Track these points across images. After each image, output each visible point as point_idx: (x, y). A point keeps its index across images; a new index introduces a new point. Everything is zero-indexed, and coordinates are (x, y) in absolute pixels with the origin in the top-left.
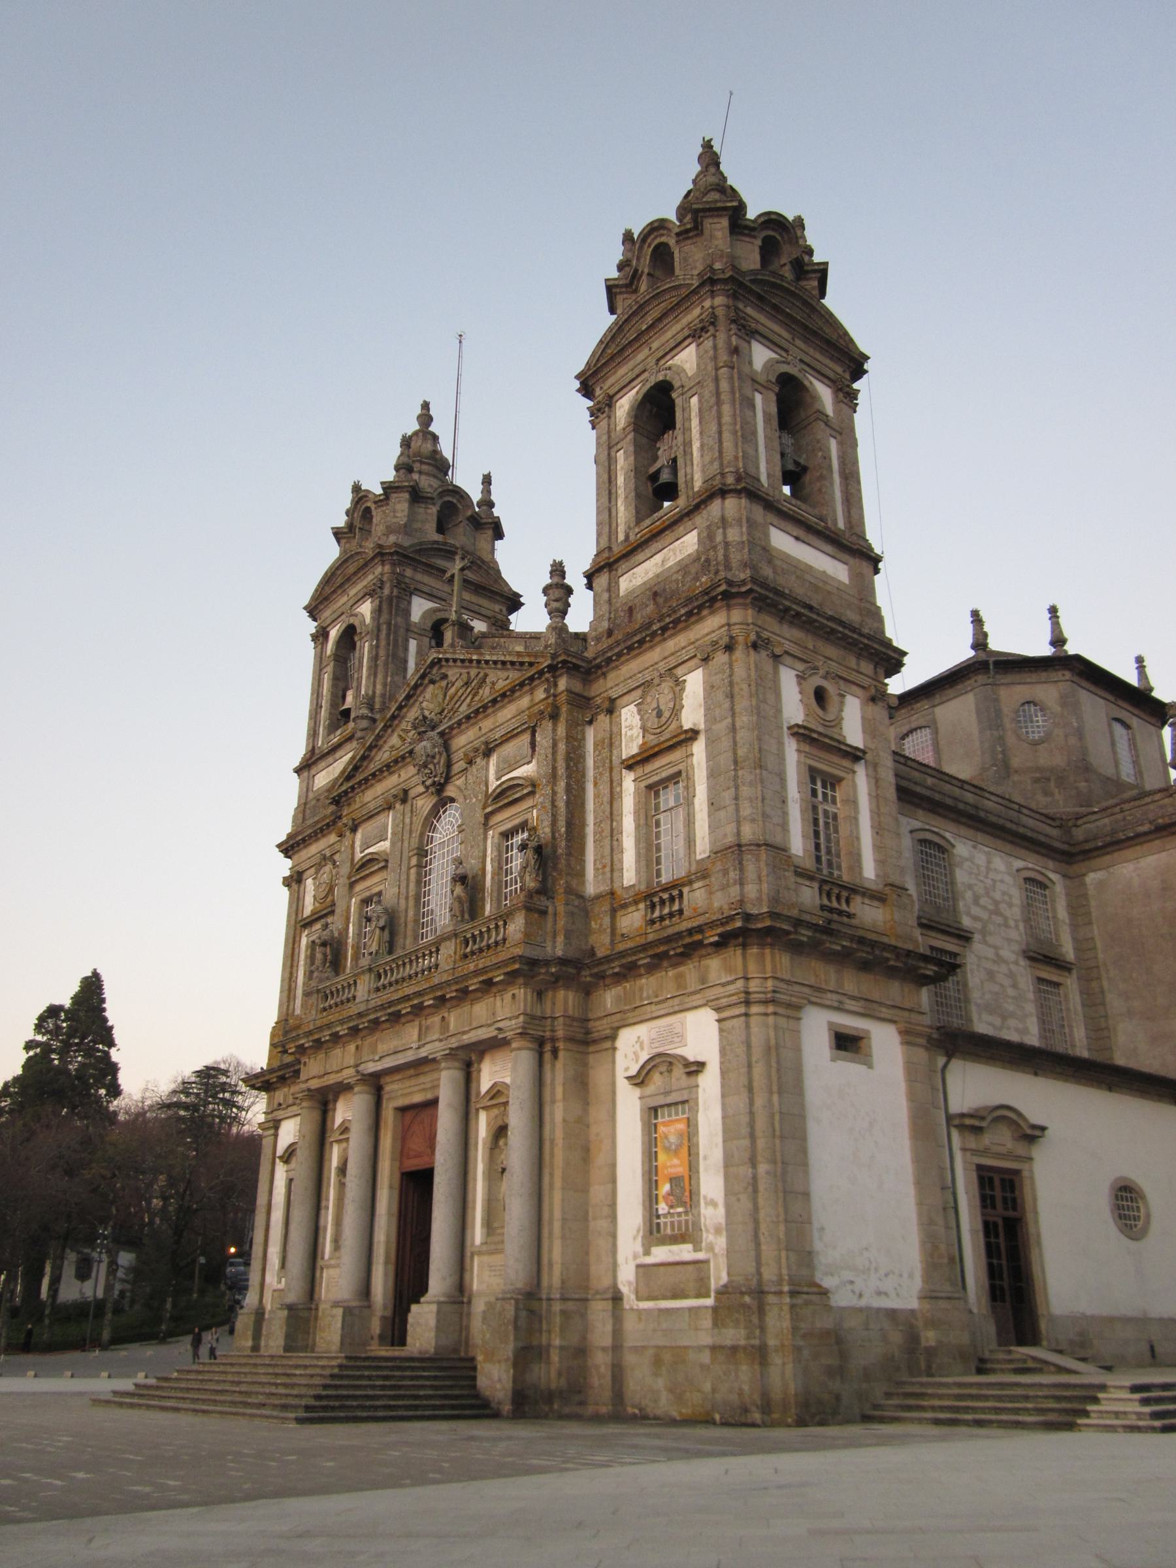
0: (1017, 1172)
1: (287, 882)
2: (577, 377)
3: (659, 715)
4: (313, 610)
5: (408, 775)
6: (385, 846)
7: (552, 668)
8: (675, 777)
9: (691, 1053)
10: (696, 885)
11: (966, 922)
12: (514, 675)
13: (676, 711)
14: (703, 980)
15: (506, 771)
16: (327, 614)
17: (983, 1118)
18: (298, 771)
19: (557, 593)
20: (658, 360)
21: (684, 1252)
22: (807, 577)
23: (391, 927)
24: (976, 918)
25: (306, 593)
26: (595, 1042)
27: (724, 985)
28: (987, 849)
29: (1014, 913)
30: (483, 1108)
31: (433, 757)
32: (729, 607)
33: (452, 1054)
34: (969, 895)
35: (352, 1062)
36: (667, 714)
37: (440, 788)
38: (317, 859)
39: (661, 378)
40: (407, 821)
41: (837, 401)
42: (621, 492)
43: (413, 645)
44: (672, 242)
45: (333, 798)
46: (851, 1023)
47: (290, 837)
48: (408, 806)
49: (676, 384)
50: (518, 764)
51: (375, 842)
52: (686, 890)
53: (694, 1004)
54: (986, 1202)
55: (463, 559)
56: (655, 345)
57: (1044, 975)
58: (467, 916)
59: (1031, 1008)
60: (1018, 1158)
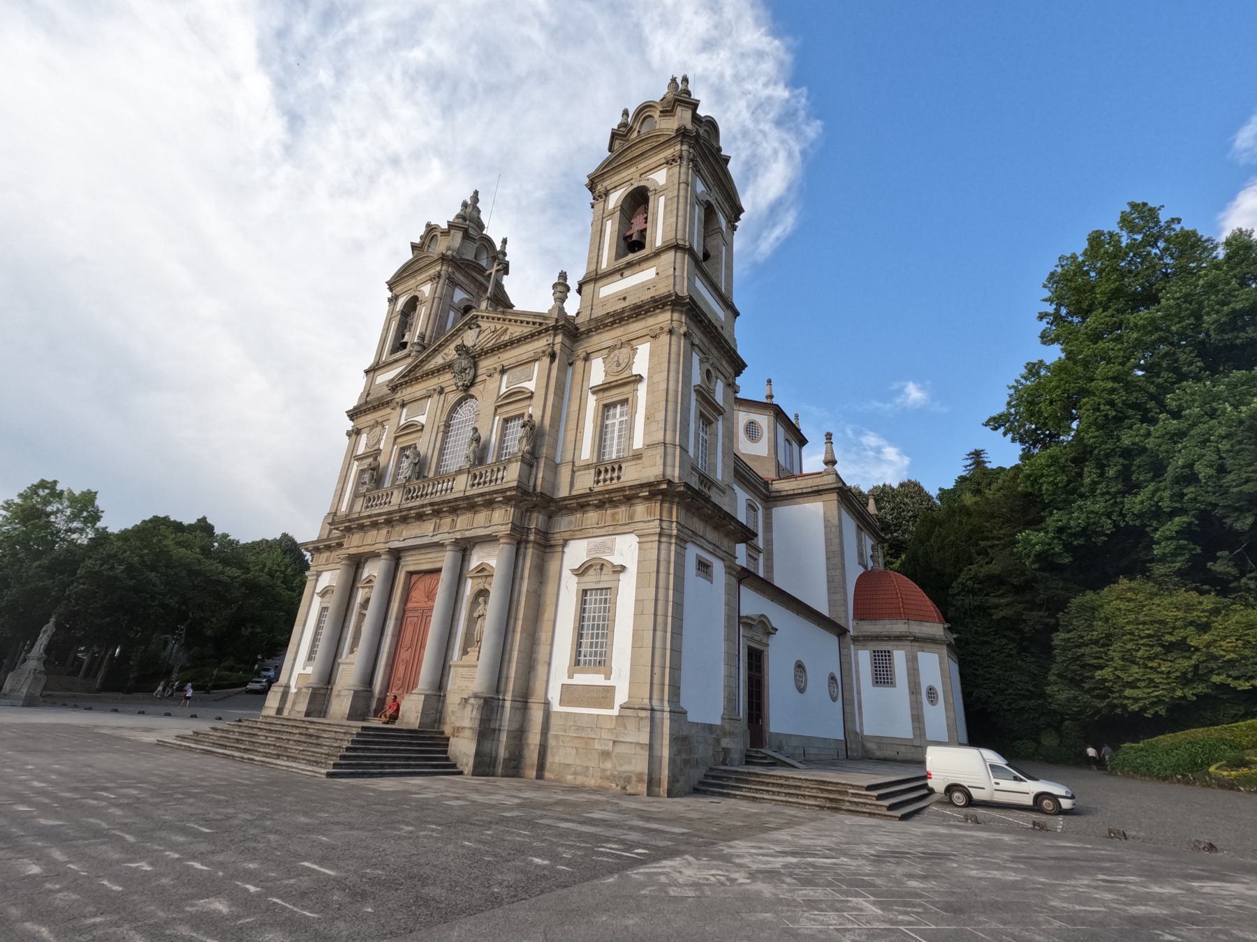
0: (763, 651)
1: (349, 434)
2: (588, 177)
3: (619, 365)
4: (392, 285)
5: (447, 379)
7: (555, 328)
8: (624, 402)
9: (616, 560)
12: (527, 330)
13: (629, 365)
14: (631, 517)
16: (398, 290)
17: (754, 620)
18: (367, 372)
19: (560, 288)
20: (641, 175)
21: (596, 679)
23: (420, 467)
25: (390, 274)
26: (552, 546)
27: (645, 522)
30: (470, 577)
31: (466, 369)
32: (673, 311)
33: (457, 542)
35: (383, 540)
36: (623, 365)
39: (642, 184)
46: (707, 557)
47: (355, 408)
48: (442, 397)
52: (623, 466)
53: (623, 531)
55: (498, 265)
56: (640, 166)
58: (477, 463)
60: (760, 642)
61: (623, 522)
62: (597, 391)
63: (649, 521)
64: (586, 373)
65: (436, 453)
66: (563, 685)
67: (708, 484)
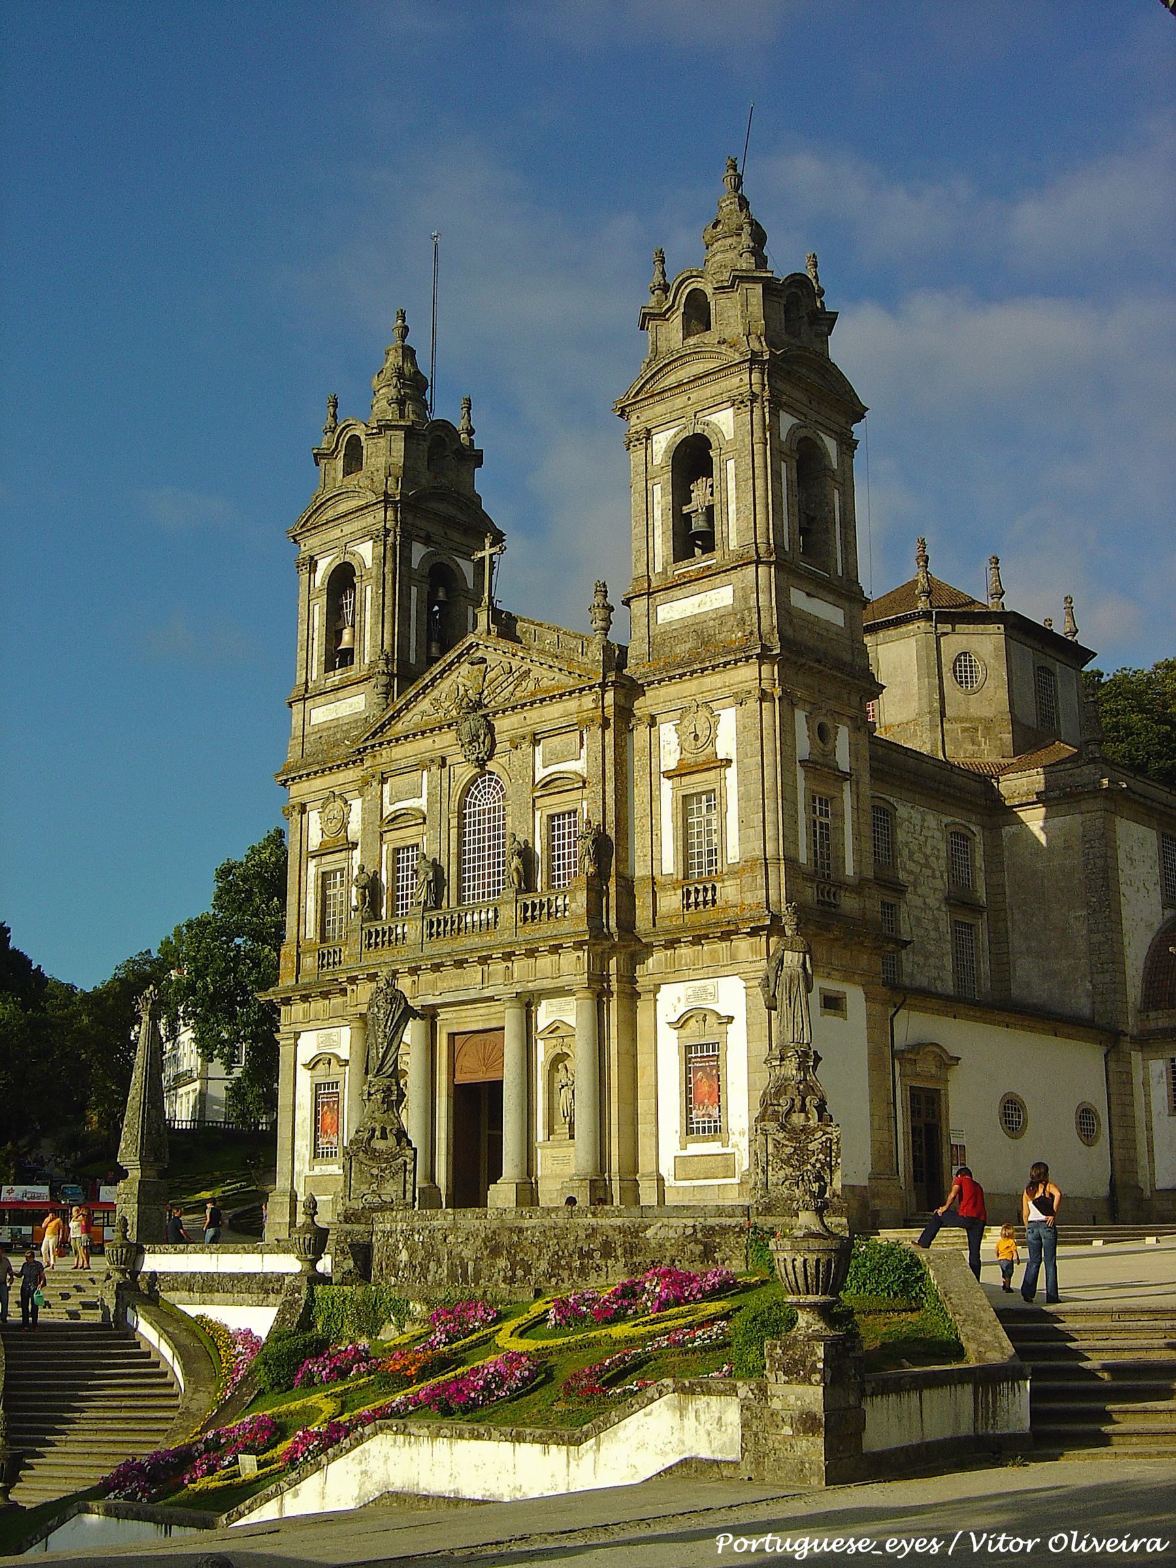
3: (696, 737)
6: (421, 803)
10: (727, 883)
11: (902, 876)
13: (712, 740)
15: (553, 762)
21: (714, 1147)
22: (817, 629)
24: (911, 872)
28: (922, 809)
29: (940, 865)
34: (906, 852)
37: (481, 764)
38: (326, 793)
40: (445, 785)
41: (841, 453)
42: (658, 524)
43: (414, 590)
44: (709, 291)
45: (358, 750)
46: (834, 986)
49: (714, 444)
50: (566, 759)
51: (408, 796)
54: (915, 1113)
57: (960, 918)
59: (948, 947)
61: (725, 963)
62: (669, 775)
63: (755, 961)
64: (652, 749)
65: (454, 860)
66: (675, 1157)
67: (833, 889)
